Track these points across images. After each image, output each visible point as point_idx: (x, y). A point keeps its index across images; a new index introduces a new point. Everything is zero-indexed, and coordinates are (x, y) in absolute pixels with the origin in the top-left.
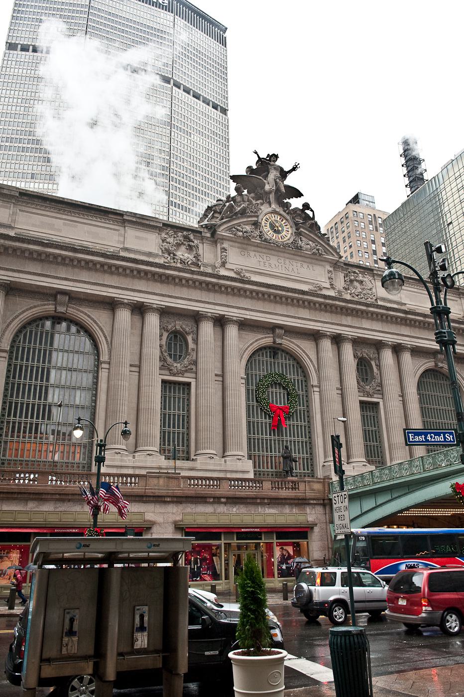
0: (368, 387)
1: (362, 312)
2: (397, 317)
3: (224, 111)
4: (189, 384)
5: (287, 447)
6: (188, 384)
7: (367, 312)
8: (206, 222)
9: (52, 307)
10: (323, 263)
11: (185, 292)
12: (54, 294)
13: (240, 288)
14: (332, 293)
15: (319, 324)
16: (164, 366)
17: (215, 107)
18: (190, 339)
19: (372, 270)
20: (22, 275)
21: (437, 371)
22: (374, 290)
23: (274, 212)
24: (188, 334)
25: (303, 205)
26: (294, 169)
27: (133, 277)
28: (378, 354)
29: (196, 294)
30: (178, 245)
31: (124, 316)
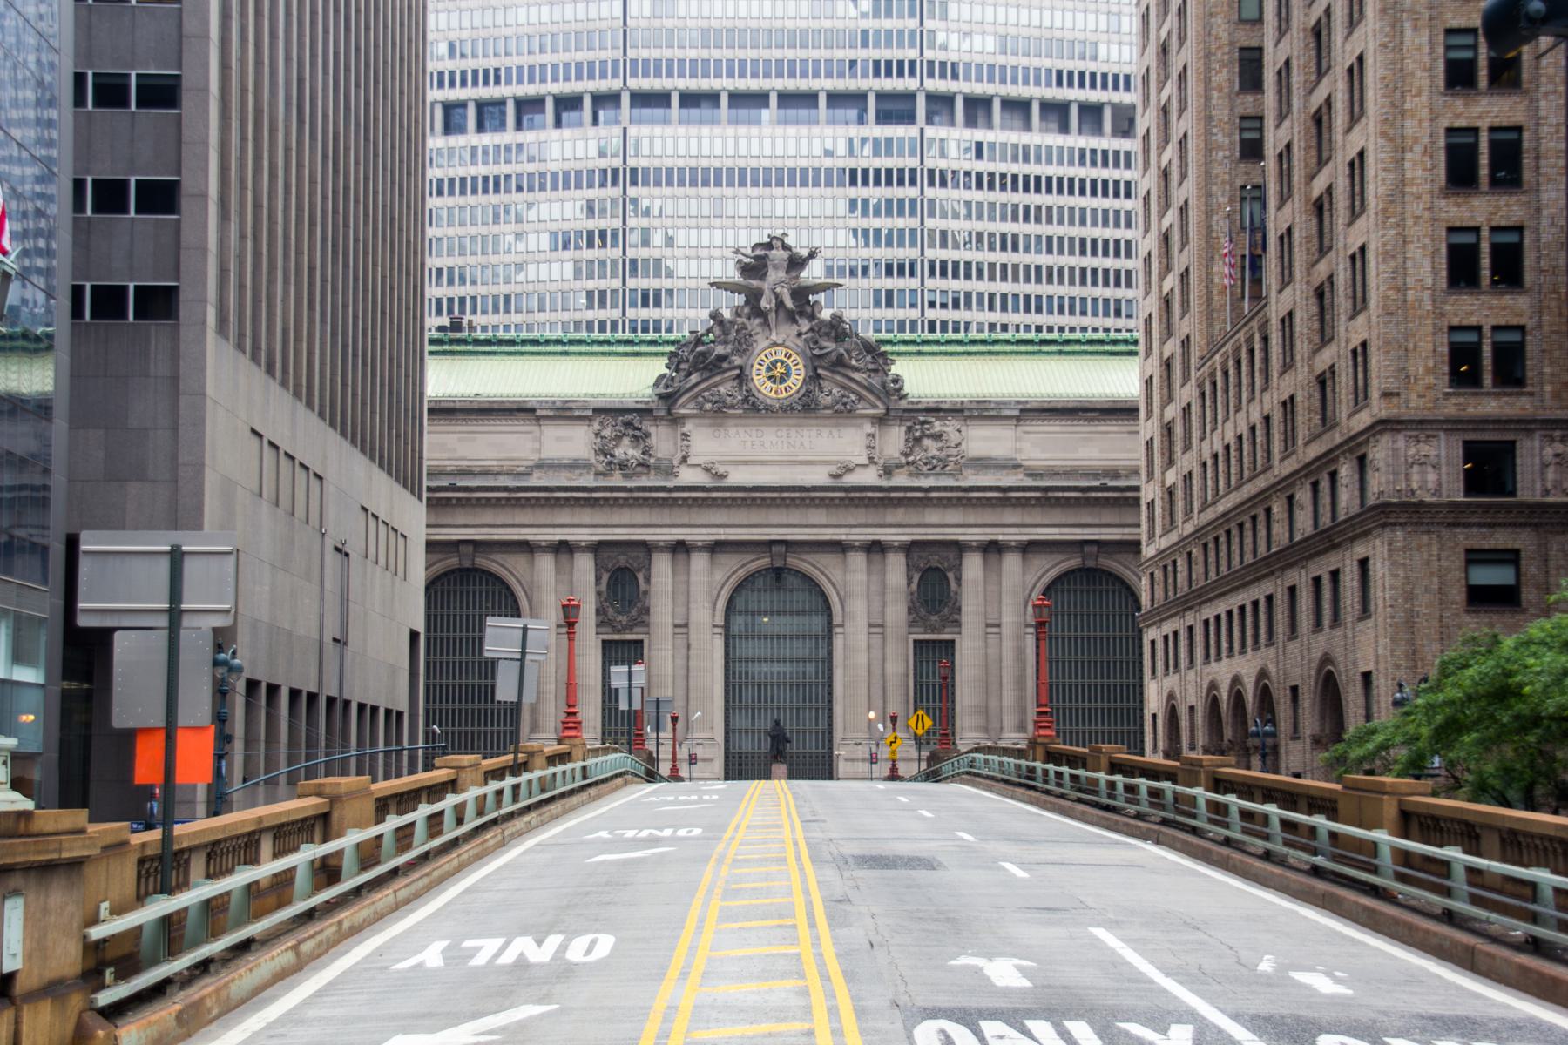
0: (934, 618)
4: (641, 641)
5: (777, 723)
6: (641, 641)
8: (661, 390)
10: (859, 421)
11: (625, 516)
15: (843, 530)
16: (603, 621)
19: (962, 411)
21: (1095, 570)
22: (964, 446)
23: (775, 344)
24: (639, 570)
26: (812, 255)
28: (960, 558)
29: (640, 516)
30: (618, 438)
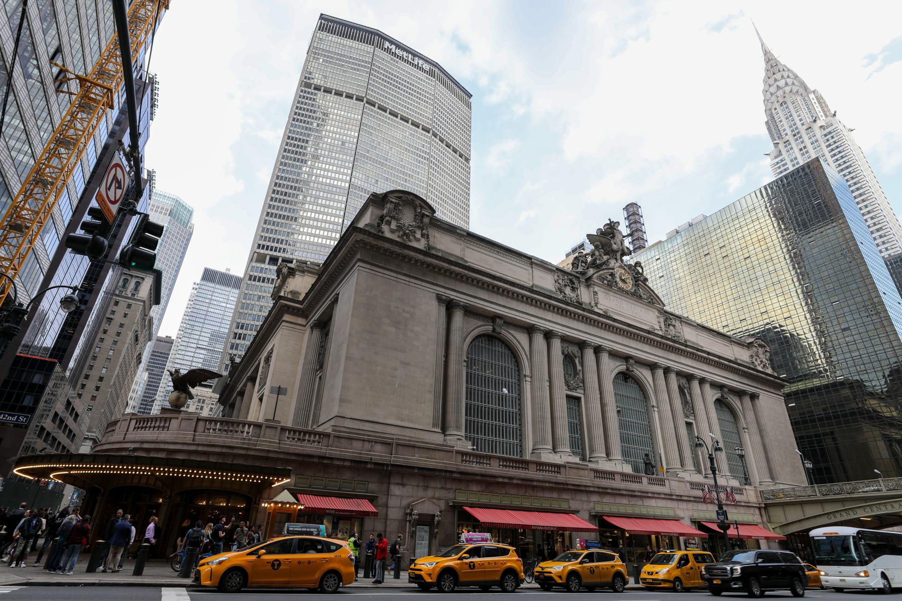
1: (682, 350)
2: (702, 357)
3: (467, 160)
6: (579, 399)
7: (685, 351)
9: (491, 328)
12: (494, 318)
13: (607, 323)
14: (660, 333)
17: (461, 156)
18: (577, 361)
20: (476, 301)
25: (636, 263)
27: (545, 309)
30: (565, 286)
31: (539, 339)
